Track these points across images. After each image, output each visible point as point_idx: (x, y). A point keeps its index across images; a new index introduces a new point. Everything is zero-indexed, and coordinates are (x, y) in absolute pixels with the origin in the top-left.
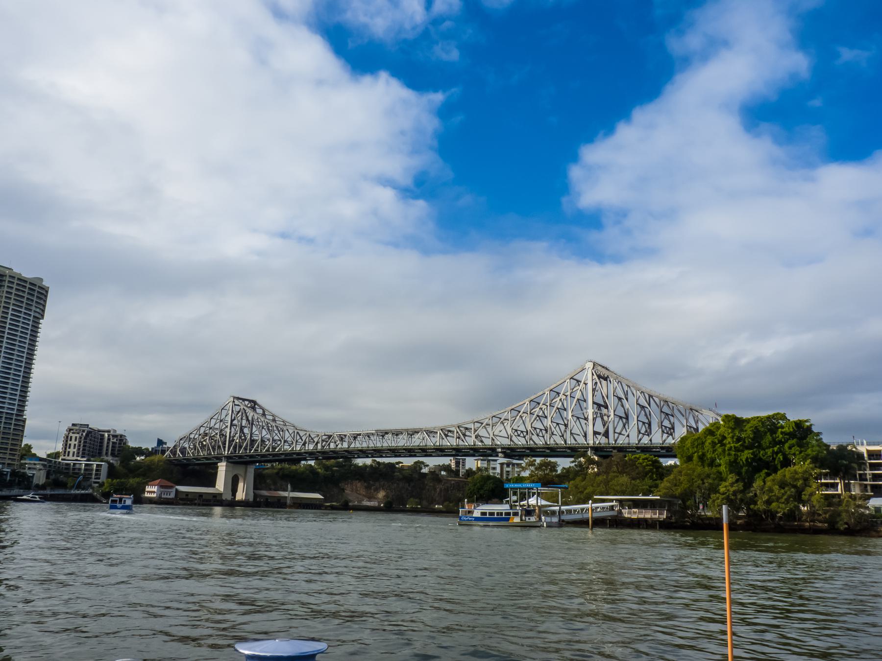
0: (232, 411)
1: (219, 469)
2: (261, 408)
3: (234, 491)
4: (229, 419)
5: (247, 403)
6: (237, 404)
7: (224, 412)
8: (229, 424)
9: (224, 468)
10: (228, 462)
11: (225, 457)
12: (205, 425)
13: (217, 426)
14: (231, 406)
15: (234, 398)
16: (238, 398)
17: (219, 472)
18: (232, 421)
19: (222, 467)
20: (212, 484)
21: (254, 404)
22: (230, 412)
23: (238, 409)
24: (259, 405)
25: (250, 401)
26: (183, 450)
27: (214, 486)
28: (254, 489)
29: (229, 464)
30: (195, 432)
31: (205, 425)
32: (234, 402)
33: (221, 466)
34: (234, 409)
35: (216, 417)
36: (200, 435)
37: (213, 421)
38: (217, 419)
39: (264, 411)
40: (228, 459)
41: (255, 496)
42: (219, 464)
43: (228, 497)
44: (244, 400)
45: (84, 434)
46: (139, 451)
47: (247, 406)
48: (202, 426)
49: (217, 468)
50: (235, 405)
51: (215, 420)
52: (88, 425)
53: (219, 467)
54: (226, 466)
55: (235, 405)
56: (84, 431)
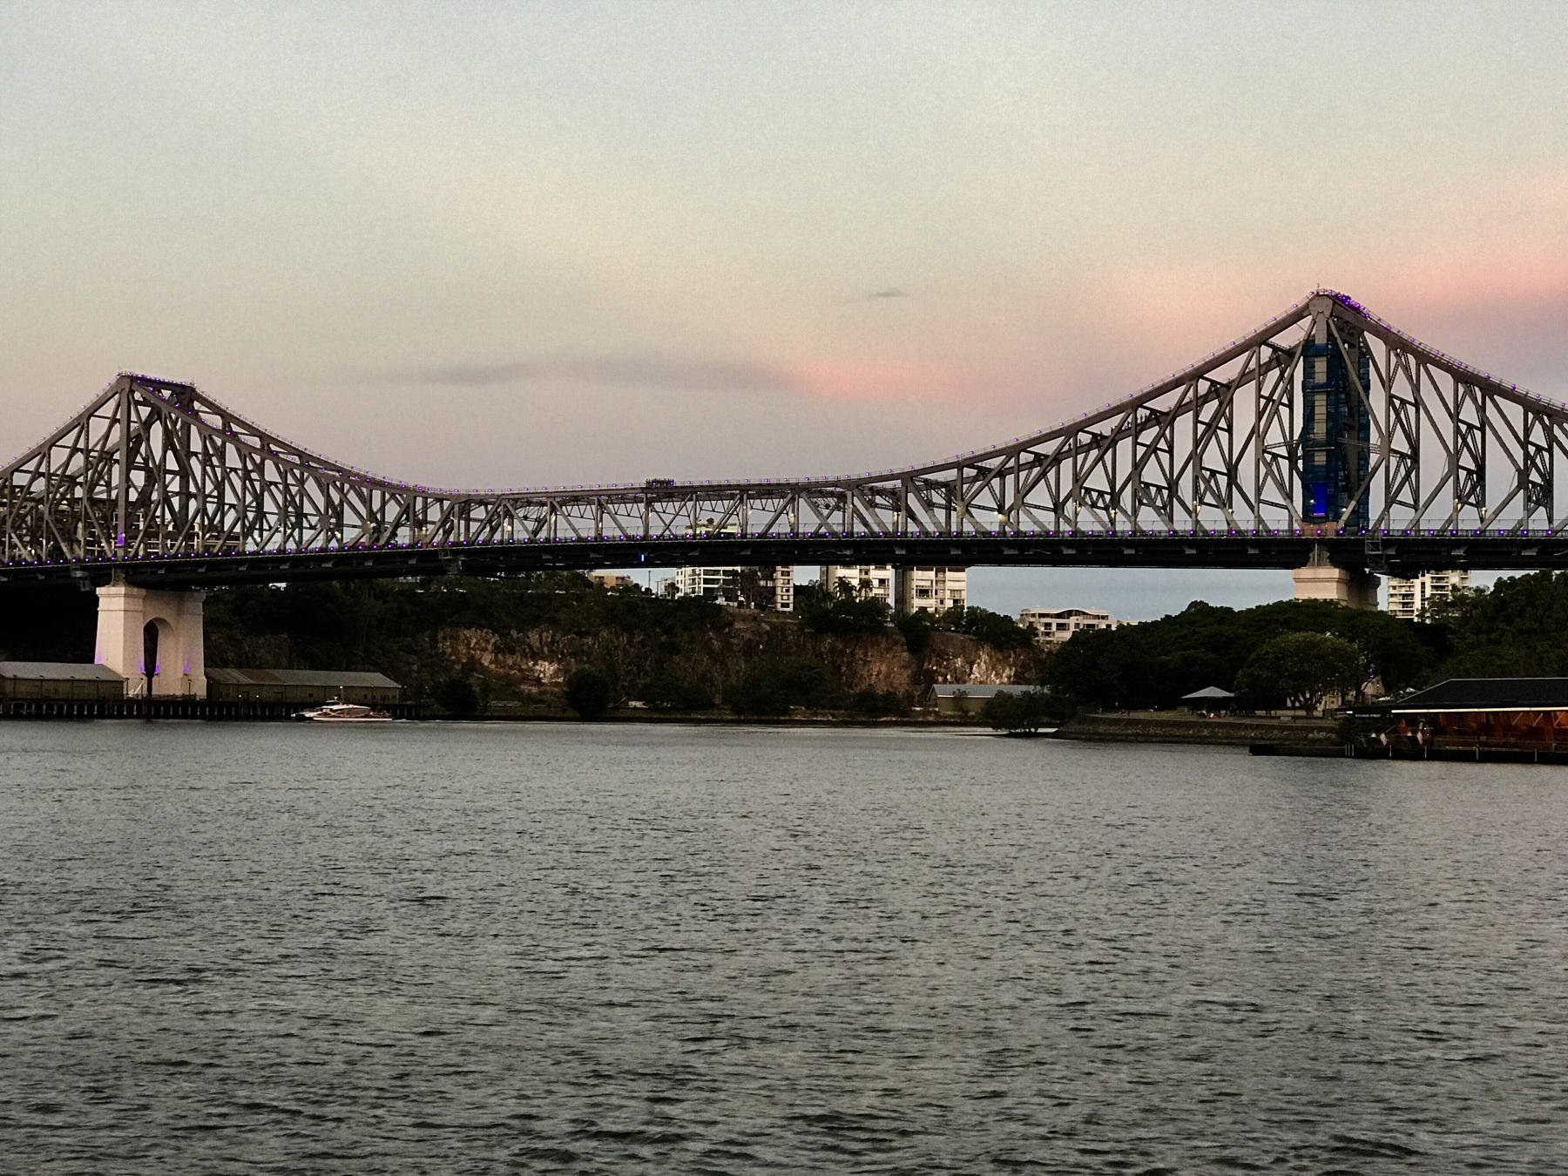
1: (103, 604)
2: (216, 410)
3: (150, 669)
5: (166, 393)
7: (98, 427)
9: (120, 603)
10: (130, 582)
11: (117, 566)
14: (124, 405)
15: (133, 379)
16: (144, 381)
17: (100, 613)
21: (185, 395)
23: (145, 411)
24: (204, 401)
27: (91, 660)
28: (210, 661)
29: (135, 590)
31: (31, 466)
32: (132, 392)
33: (109, 596)
34: (134, 417)
35: (69, 440)
37: (58, 456)
39: (226, 424)
40: (127, 573)
41: (211, 686)
42: (99, 591)
43: (135, 690)
44: (159, 385)
48: (17, 470)
49: (96, 600)
50: (137, 403)
53: (101, 600)
54: (126, 596)
55: (137, 403)
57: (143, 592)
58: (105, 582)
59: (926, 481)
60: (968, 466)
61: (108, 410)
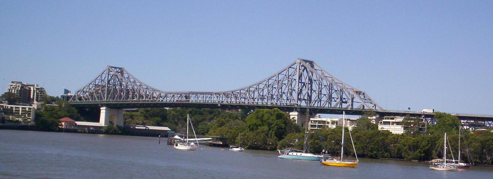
0: (108, 75)
4: (106, 79)
5: (118, 69)
6: (111, 70)
7: (104, 75)
8: (107, 83)
9: (104, 111)
12: (93, 83)
13: (100, 84)
18: (109, 81)
19: (103, 111)
20: (98, 120)
22: (107, 76)
23: (112, 73)
25: (120, 69)
26: (80, 99)
30: (87, 87)
35: (99, 78)
36: (89, 89)
38: (100, 80)
42: (101, 108)
44: (116, 68)
45: (19, 88)
46: (53, 99)
47: (117, 72)
48: (91, 84)
49: (100, 110)
51: (98, 80)
52: (21, 82)
53: (101, 110)
54: (106, 109)
56: (19, 86)
57: (109, 109)
58: (102, 106)
59: (237, 93)
60: (241, 90)
61: (105, 73)
